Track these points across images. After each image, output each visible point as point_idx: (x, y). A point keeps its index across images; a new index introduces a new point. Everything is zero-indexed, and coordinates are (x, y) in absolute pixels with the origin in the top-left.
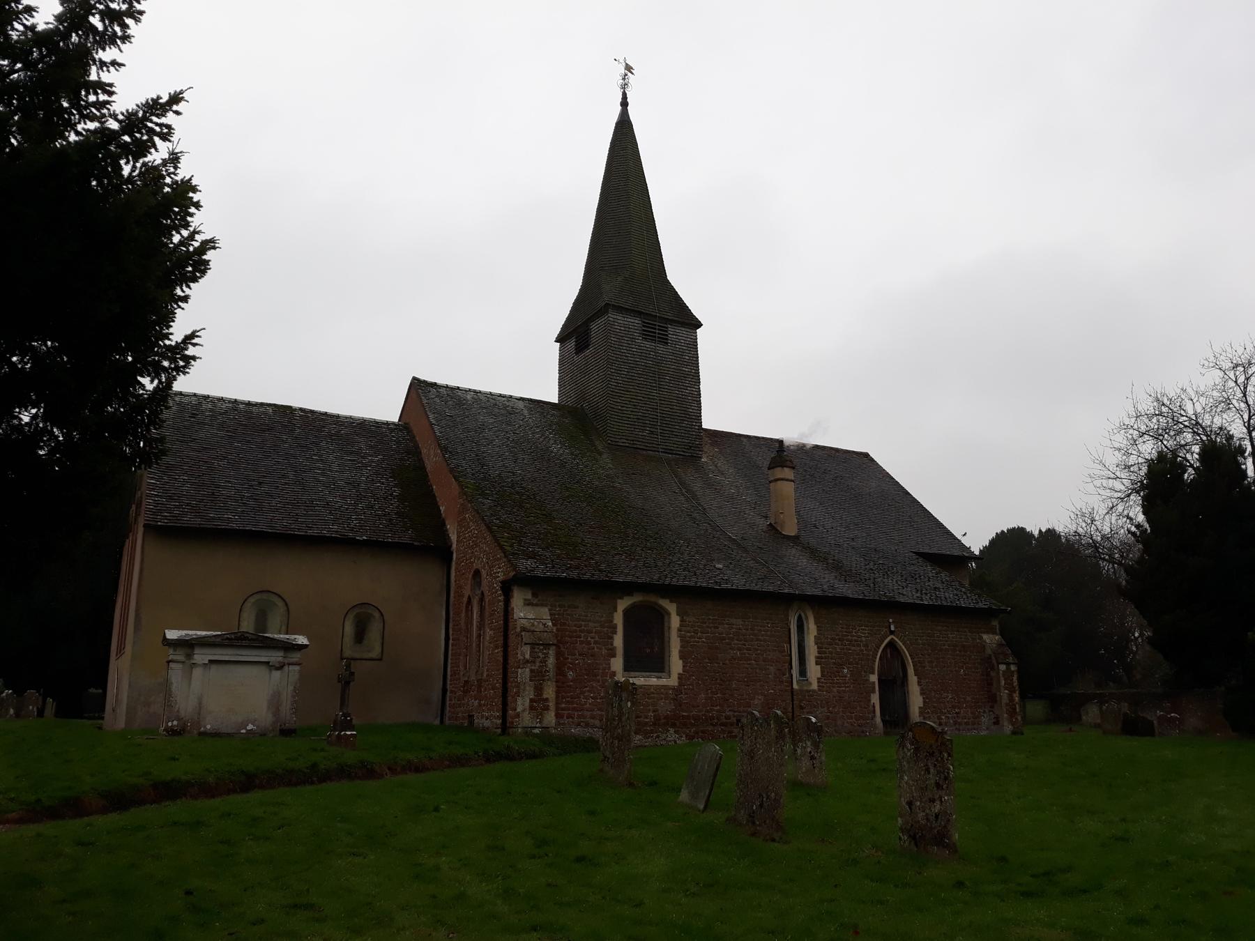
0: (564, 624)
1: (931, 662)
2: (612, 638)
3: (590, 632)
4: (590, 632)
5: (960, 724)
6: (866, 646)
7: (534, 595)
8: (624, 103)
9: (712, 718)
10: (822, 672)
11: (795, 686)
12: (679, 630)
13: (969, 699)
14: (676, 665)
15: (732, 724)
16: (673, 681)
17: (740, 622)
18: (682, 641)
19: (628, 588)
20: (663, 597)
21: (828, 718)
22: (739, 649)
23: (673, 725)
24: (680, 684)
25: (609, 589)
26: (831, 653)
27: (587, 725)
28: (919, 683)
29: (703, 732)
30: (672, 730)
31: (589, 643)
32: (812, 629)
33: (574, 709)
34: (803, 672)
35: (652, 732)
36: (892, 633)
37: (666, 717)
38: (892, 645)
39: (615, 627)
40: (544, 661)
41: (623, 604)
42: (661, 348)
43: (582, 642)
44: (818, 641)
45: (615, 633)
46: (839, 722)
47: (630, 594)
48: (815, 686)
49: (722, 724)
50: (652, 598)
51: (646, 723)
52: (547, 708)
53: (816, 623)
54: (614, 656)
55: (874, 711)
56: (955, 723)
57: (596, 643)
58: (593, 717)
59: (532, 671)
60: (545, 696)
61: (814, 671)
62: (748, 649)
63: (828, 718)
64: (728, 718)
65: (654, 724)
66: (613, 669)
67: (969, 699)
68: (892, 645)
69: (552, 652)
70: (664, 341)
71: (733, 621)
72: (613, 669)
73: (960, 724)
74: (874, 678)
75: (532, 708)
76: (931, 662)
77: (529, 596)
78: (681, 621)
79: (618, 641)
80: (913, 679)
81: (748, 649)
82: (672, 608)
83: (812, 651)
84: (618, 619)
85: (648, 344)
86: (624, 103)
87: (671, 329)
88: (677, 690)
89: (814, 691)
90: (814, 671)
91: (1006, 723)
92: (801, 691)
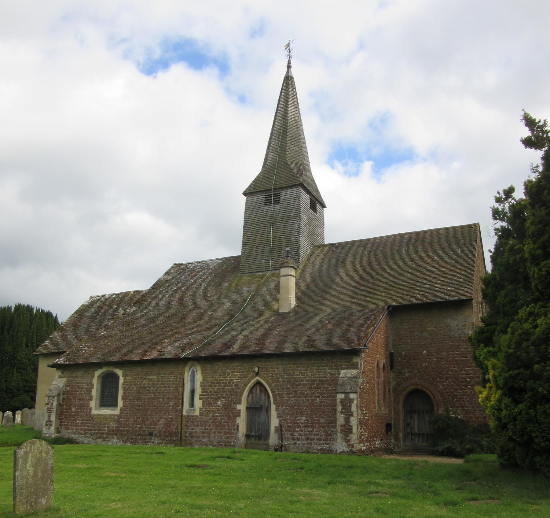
0: (73, 385)
1: (287, 394)
2: (91, 391)
3: (83, 388)
4: (83, 388)
5: (312, 439)
6: (237, 385)
7: (63, 373)
8: (289, 67)
9: (136, 431)
10: (203, 404)
11: (184, 413)
12: (123, 384)
13: (322, 420)
14: (120, 403)
15: (146, 435)
16: (116, 412)
17: (155, 377)
18: (124, 390)
19: (98, 365)
20: (116, 368)
21: (204, 433)
22: (154, 393)
23: (116, 435)
24: (121, 413)
25: (89, 366)
26: (210, 392)
27: (79, 433)
28: (277, 409)
29: (131, 439)
30: (115, 437)
31: (82, 394)
32: (199, 377)
33: (74, 426)
34: (192, 404)
35: (106, 438)
36: (257, 374)
37: (113, 431)
38: (258, 383)
39: (93, 385)
40: (52, 404)
41: (98, 373)
42: (277, 206)
43: (79, 394)
44: (202, 385)
45: (93, 388)
46: (212, 435)
47: (101, 368)
48: (197, 413)
49: (141, 435)
50: (111, 369)
51: (103, 434)
52: (51, 425)
53: (202, 373)
54: (91, 399)
55: (238, 429)
56: (308, 439)
57: (85, 394)
58: (81, 429)
59: (48, 408)
60: (51, 420)
61: (198, 403)
62: (159, 393)
63: (204, 433)
64: (144, 431)
65: (107, 434)
66: (91, 406)
67: (322, 420)
68: (258, 383)
69: (56, 398)
70: (277, 202)
71: (152, 377)
72: (91, 406)
73: (312, 439)
74: (242, 407)
75: (46, 425)
76: (287, 394)
77: (60, 373)
78: (125, 379)
79: (95, 392)
80: (273, 407)
81: (159, 393)
82: (119, 372)
83: (198, 391)
84: (95, 381)
85: (268, 208)
86: (289, 67)
87: (283, 193)
88: (120, 416)
89: (196, 416)
90: (198, 403)
91: (339, 440)
92: (188, 416)
